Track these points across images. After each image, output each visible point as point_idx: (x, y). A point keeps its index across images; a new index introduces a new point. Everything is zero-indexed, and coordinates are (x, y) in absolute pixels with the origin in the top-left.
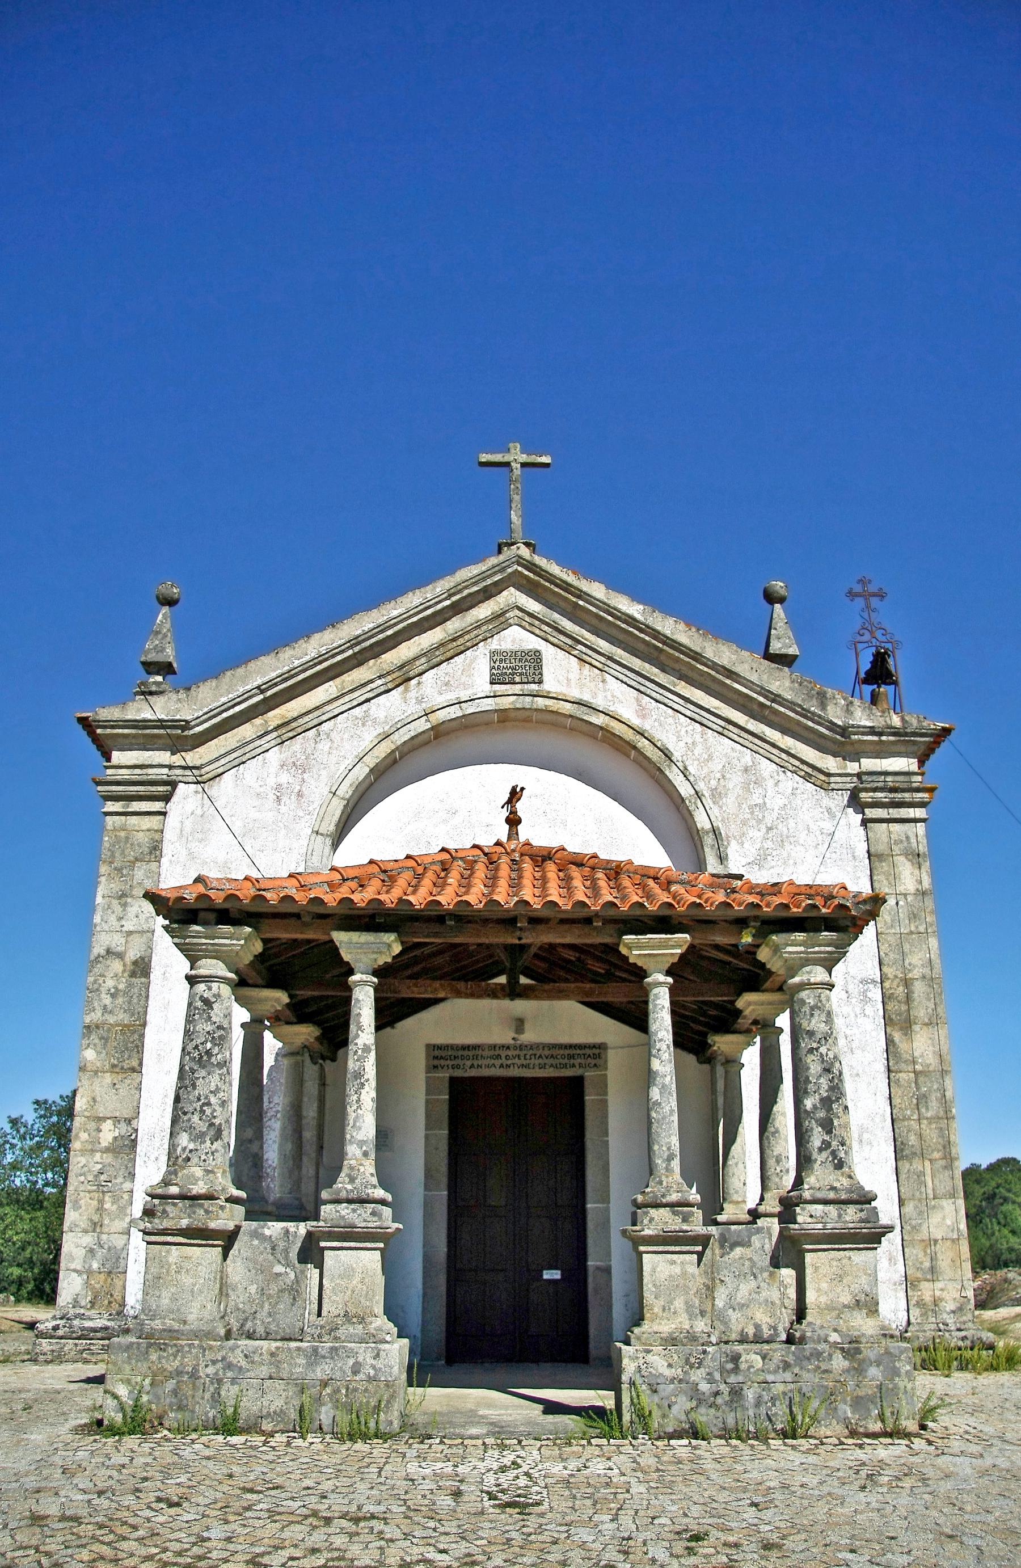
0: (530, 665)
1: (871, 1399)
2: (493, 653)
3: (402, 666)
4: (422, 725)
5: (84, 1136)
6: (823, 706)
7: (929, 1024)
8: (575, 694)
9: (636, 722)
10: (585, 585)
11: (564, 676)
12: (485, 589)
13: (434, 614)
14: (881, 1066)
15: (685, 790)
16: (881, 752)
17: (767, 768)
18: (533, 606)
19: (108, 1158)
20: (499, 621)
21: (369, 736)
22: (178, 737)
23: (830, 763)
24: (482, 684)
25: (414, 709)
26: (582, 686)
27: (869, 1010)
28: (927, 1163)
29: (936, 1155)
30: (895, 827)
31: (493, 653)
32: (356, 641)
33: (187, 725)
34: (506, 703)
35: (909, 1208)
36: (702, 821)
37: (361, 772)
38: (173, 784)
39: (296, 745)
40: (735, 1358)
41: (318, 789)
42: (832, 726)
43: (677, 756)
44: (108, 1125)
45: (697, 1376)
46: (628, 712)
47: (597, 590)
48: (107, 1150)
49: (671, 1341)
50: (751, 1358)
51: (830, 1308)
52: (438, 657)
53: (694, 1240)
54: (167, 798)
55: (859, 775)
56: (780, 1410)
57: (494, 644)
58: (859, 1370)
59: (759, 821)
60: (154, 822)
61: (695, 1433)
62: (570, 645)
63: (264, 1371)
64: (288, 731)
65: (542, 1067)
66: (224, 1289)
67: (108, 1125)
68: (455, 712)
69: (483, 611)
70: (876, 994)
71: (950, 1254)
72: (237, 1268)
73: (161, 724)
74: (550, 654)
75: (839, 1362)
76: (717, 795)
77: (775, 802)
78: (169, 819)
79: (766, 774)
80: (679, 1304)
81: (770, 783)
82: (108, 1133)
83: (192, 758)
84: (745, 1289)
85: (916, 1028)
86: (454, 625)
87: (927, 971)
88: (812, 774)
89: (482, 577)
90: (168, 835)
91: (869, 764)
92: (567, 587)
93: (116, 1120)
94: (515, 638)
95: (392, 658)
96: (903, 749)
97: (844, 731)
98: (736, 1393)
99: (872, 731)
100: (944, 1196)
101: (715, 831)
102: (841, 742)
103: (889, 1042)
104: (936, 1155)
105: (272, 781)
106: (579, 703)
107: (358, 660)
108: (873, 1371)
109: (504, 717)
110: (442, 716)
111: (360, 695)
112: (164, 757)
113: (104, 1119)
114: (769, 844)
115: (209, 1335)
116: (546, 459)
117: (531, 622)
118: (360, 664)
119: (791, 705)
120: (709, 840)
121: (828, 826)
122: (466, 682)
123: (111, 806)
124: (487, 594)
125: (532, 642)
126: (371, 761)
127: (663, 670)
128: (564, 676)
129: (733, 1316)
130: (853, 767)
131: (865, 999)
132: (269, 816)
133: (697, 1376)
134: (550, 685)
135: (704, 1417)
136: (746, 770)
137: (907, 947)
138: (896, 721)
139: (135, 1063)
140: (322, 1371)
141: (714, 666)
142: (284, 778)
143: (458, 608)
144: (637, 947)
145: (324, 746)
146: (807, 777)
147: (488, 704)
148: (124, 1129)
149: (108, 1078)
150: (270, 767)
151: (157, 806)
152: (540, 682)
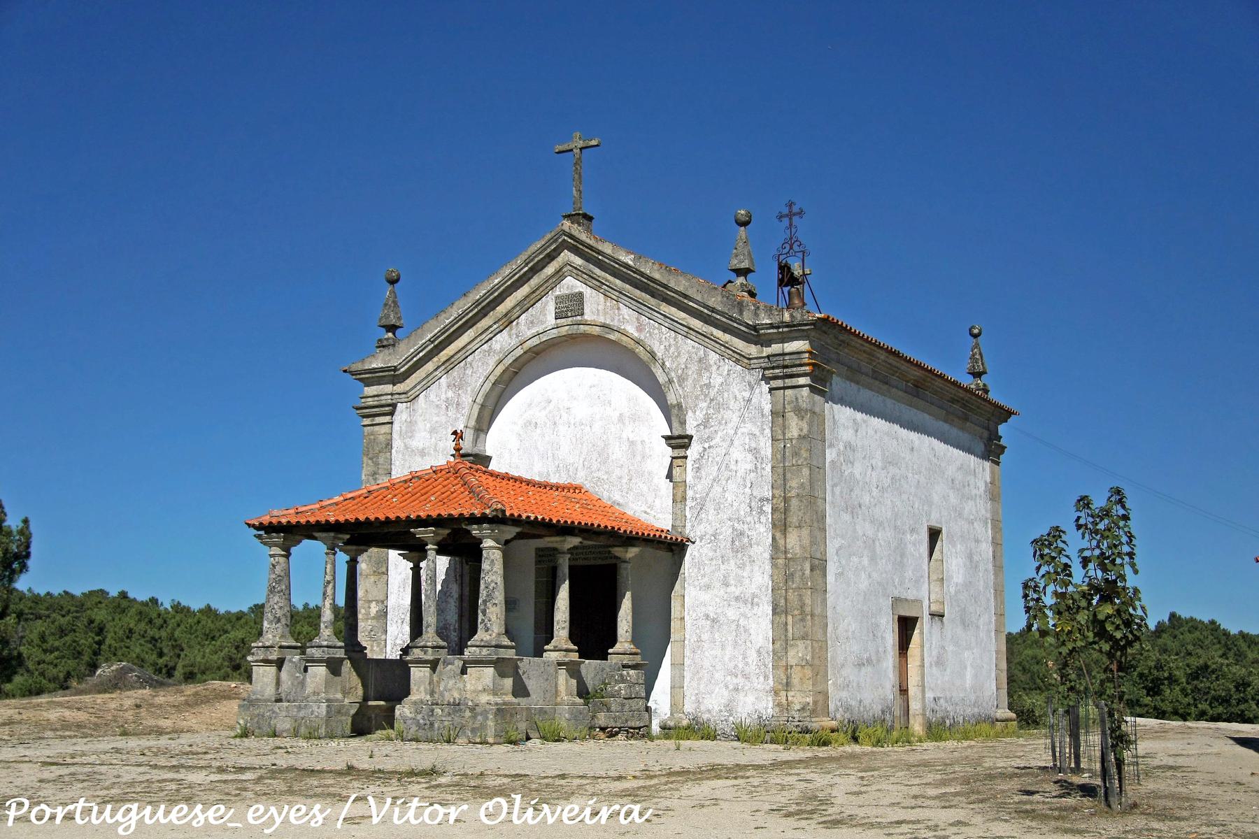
1: (477, 729)
2: (557, 297)
3: (506, 315)
4: (519, 352)
5: (363, 611)
6: (741, 312)
7: (800, 527)
8: (601, 320)
9: (636, 334)
10: (600, 247)
11: (597, 308)
12: (548, 255)
13: (520, 277)
14: (767, 555)
15: (662, 378)
16: (784, 339)
17: (713, 357)
18: (578, 261)
19: (374, 623)
20: (559, 275)
21: (492, 362)
22: (394, 376)
23: (753, 350)
24: (551, 320)
26: (605, 313)
27: (763, 519)
28: (790, 618)
29: (796, 612)
30: (788, 392)
31: (557, 297)
33: (395, 369)
34: (564, 331)
35: (778, 645)
36: (672, 399)
37: (488, 386)
38: (394, 406)
39: (455, 373)
40: (432, 711)
41: (467, 399)
42: (747, 326)
43: (659, 355)
44: (373, 605)
45: (419, 717)
46: (631, 330)
47: (607, 248)
48: (373, 618)
49: (415, 703)
50: (438, 711)
51: (474, 691)
52: (525, 305)
53: (426, 662)
54: (392, 414)
55: (768, 357)
56: (445, 733)
57: (557, 292)
58: (474, 717)
59: (706, 396)
60: (385, 429)
61: (417, 740)
62: (598, 285)
63: (284, 714)
64: (449, 365)
65: (595, 559)
66: (278, 683)
67: (373, 605)
68: (536, 341)
69: (550, 270)
70: (768, 508)
71: (800, 675)
72: (284, 675)
73: (382, 370)
74: (588, 292)
75: (468, 714)
76: (682, 380)
77: (717, 380)
78: (396, 426)
79: (712, 362)
80: (422, 688)
81: (714, 368)
82: (374, 609)
83: (400, 388)
84: (451, 683)
85: (790, 529)
86: (535, 281)
87: (800, 491)
88: (740, 358)
89: (543, 248)
90: (395, 436)
91: (776, 348)
92: (591, 247)
93: (377, 602)
94: (571, 284)
95: (502, 309)
96: (796, 334)
97: (754, 328)
98: (432, 724)
99: (771, 326)
100: (799, 639)
101: (679, 406)
102: (755, 335)
103: (774, 538)
104: (796, 612)
105: (443, 397)
106: (603, 326)
107: (483, 313)
108: (479, 718)
109: (572, 338)
111: (485, 337)
112: (388, 388)
113: (370, 602)
114: (711, 411)
115: (269, 700)
116: (594, 143)
117: (578, 273)
118: (485, 315)
119: (722, 314)
120: (675, 411)
121: (747, 395)
122: (542, 320)
123: (367, 421)
124: (551, 257)
125: (579, 287)
126: (492, 379)
127: (653, 296)
128: (598, 309)
129: (446, 694)
130: (767, 351)
131: (762, 512)
132: (443, 419)
133: (419, 717)
134: (588, 316)
135: (421, 734)
136: (700, 360)
137: (788, 475)
138: (787, 317)
139: (384, 570)
140: (302, 714)
141: (676, 292)
142: (450, 394)
143: (535, 270)
144: (421, 533)
145: (469, 372)
146: (737, 362)
148: (381, 607)
149: (372, 579)
150: (441, 390)
151: (387, 419)
152: (582, 314)
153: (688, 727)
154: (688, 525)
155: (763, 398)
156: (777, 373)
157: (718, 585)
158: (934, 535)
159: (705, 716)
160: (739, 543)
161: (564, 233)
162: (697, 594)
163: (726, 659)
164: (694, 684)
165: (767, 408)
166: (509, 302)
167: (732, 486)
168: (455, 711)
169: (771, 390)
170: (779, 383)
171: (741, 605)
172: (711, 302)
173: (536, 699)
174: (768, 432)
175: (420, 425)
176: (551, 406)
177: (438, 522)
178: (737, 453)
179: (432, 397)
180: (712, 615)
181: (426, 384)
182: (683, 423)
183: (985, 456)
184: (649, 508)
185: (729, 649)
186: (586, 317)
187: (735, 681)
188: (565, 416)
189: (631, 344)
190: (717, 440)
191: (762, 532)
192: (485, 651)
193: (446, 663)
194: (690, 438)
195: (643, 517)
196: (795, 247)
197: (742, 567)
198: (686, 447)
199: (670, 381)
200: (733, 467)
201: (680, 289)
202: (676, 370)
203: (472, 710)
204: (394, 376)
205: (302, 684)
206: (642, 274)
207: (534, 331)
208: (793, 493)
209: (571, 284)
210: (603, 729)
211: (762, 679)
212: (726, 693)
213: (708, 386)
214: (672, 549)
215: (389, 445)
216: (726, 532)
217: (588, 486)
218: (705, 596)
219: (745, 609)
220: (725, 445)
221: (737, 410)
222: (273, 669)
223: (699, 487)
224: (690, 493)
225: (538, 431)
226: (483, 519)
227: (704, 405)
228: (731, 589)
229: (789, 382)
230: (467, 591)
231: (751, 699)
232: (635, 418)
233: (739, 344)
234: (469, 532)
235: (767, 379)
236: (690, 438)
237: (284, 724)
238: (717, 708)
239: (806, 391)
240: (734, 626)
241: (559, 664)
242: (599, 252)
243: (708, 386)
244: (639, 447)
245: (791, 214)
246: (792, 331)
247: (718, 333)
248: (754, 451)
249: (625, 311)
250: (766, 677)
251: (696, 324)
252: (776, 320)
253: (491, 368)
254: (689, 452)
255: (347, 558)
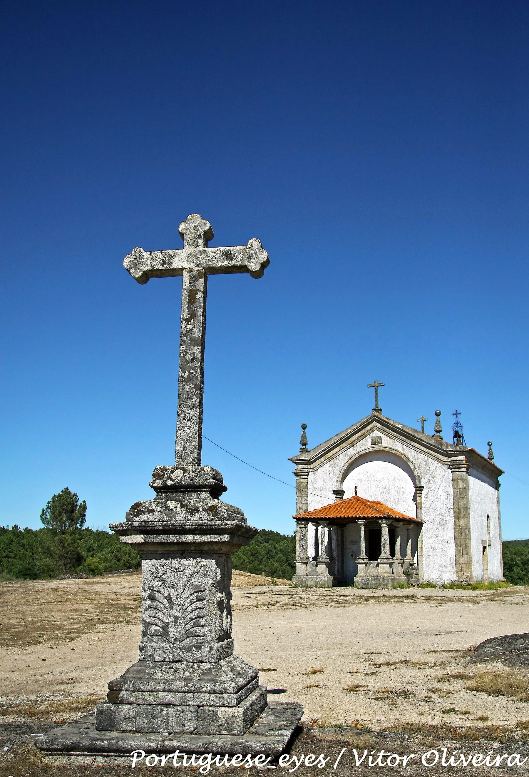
0: (377, 441)
4: (357, 456)
6: (442, 446)
7: (464, 518)
8: (389, 446)
9: (402, 451)
11: (387, 442)
14: (453, 526)
15: (412, 467)
20: (372, 430)
21: (347, 458)
22: (308, 462)
23: (445, 458)
24: (369, 445)
25: (355, 452)
26: (390, 444)
27: (450, 515)
32: (342, 438)
33: (310, 460)
34: (374, 449)
35: (457, 557)
36: (416, 474)
37: (346, 467)
38: (309, 472)
41: (337, 471)
42: (444, 451)
43: (411, 459)
45: (363, 581)
46: (400, 450)
49: (361, 576)
52: (360, 439)
53: (364, 563)
54: (308, 475)
57: (371, 435)
58: (384, 581)
62: (387, 434)
64: (330, 459)
68: (363, 452)
69: (369, 428)
70: (452, 511)
72: (308, 567)
73: (305, 460)
74: (383, 436)
75: (381, 580)
76: (419, 468)
77: (432, 468)
78: (309, 480)
84: (372, 570)
86: (363, 431)
91: (453, 458)
94: (376, 433)
97: (446, 451)
98: (368, 583)
99: (452, 451)
101: (418, 476)
102: (447, 454)
103: (455, 522)
105: (328, 470)
107: (343, 442)
110: (361, 453)
112: (306, 466)
117: (379, 429)
120: (417, 478)
121: (443, 473)
122: (366, 445)
124: (369, 424)
126: (347, 464)
128: (387, 442)
130: (450, 459)
131: (450, 513)
132: (328, 478)
133: (363, 581)
134: (383, 444)
135: (364, 586)
138: (458, 448)
142: (330, 469)
145: (338, 462)
146: (439, 462)
147: (370, 450)
150: (327, 467)
151: (306, 477)
153: (426, 584)
154: (423, 517)
155: (449, 474)
156: (454, 466)
157: (435, 537)
158: (488, 516)
159: (432, 581)
160: (442, 523)
161: (375, 416)
162: (426, 538)
163: (439, 561)
164: (427, 569)
165: (451, 478)
166: (353, 438)
167: (439, 504)
168: (376, 579)
169: (452, 472)
170: (455, 470)
171: (443, 543)
172: (431, 442)
173: (395, 575)
174: (451, 486)
175: (319, 480)
176: (368, 474)
177: (364, 518)
178: (440, 493)
179: (323, 470)
180: (433, 547)
181: (322, 465)
182: (420, 482)
183: (496, 489)
184: (408, 510)
185: (439, 559)
186: (383, 445)
187: (442, 568)
188: (373, 478)
189: (401, 455)
190: (433, 488)
191: (450, 520)
192: (386, 560)
193: (370, 564)
194: (423, 487)
195: (404, 513)
196: (459, 424)
197: (443, 531)
198: (422, 490)
199: (415, 468)
200: (439, 497)
201: (420, 437)
202: (417, 464)
203: (383, 578)
204: (308, 462)
205: (315, 570)
206: (405, 431)
207: (363, 448)
208: (461, 507)
209: (376, 433)
210: (412, 585)
211: (451, 568)
212: (439, 573)
213: (429, 470)
214: (418, 525)
215: (307, 486)
216: (437, 519)
217: (382, 502)
218: (430, 541)
219: (444, 545)
220: (436, 490)
221: (439, 478)
222: (305, 565)
223: (427, 504)
224: (423, 506)
225: (363, 482)
226: (381, 518)
227: (428, 476)
228: (440, 538)
229: (458, 470)
230: (340, 538)
231: (448, 574)
232: (399, 479)
233: (440, 456)
234: (378, 522)
235: (451, 469)
236: (423, 487)
237: (311, 583)
238: (436, 578)
239: (464, 473)
240: (441, 550)
241: (399, 564)
242: (388, 423)
243: (429, 470)
244: (402, 490)
245: (457, 414)
246: (460, 453)
247: (433, 452)
248: (447, 492)
249: (397, 443)
250: (453, 567)
251: (424, 449)
252: (454, 449)
253: (346, 460)
254: (423, 492)
255: (315, 528)
